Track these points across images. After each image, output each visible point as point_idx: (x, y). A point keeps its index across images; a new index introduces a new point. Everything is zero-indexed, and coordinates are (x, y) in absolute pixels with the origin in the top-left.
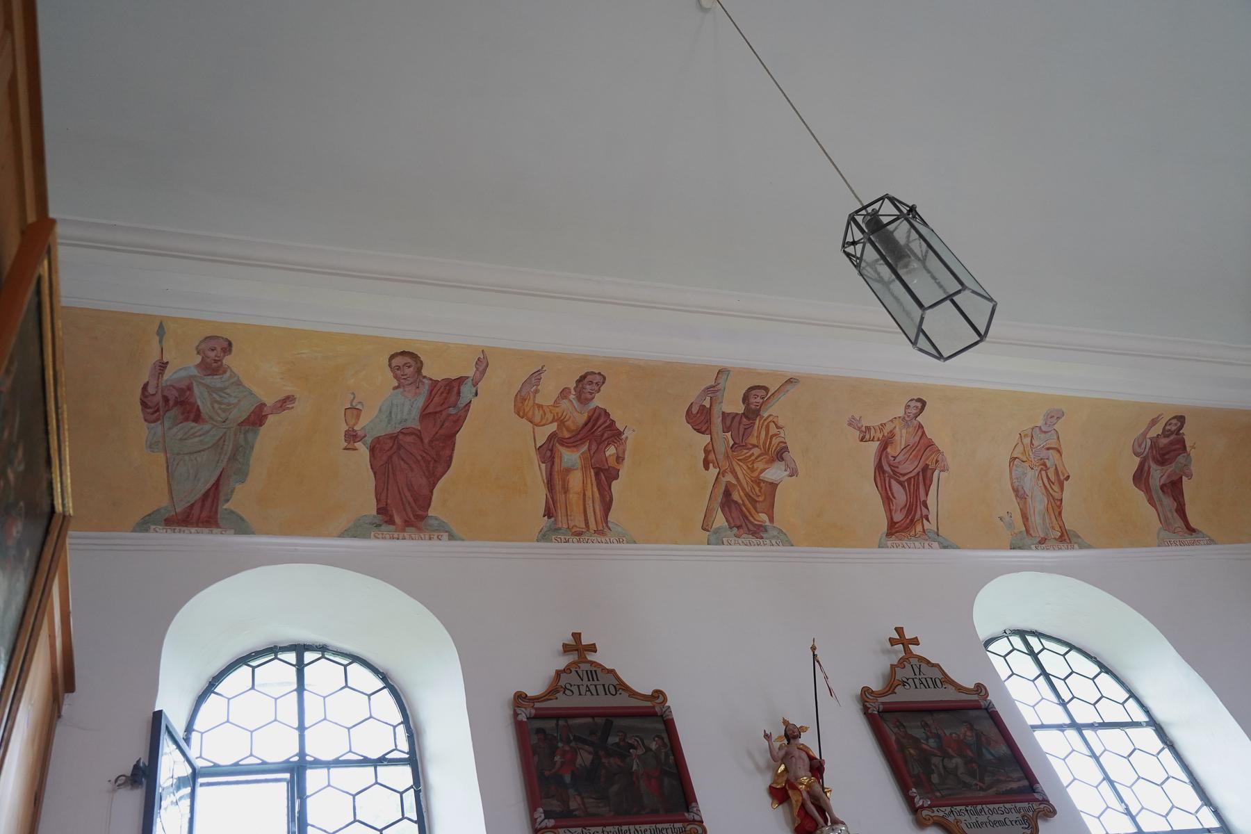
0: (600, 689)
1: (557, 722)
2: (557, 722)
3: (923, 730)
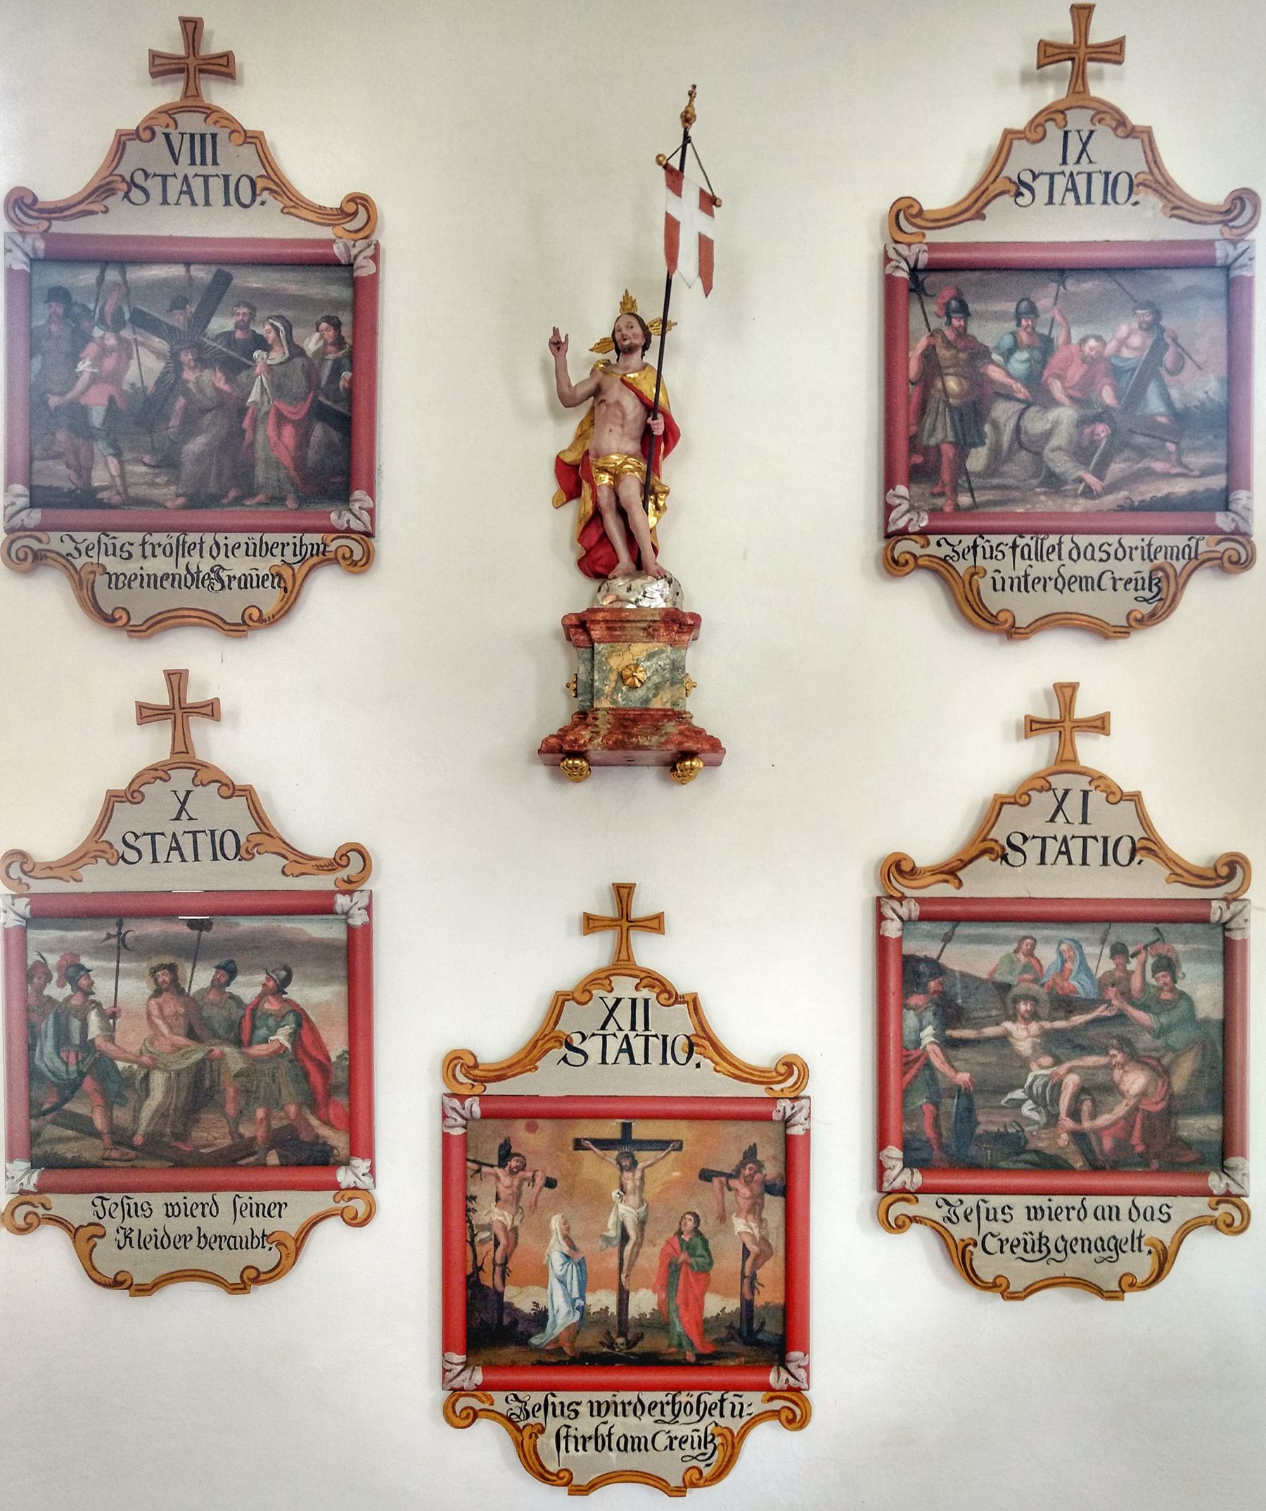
0: (216, 185)
1: (102, 272)
2: (102, 272)
3: (1012, 325)
